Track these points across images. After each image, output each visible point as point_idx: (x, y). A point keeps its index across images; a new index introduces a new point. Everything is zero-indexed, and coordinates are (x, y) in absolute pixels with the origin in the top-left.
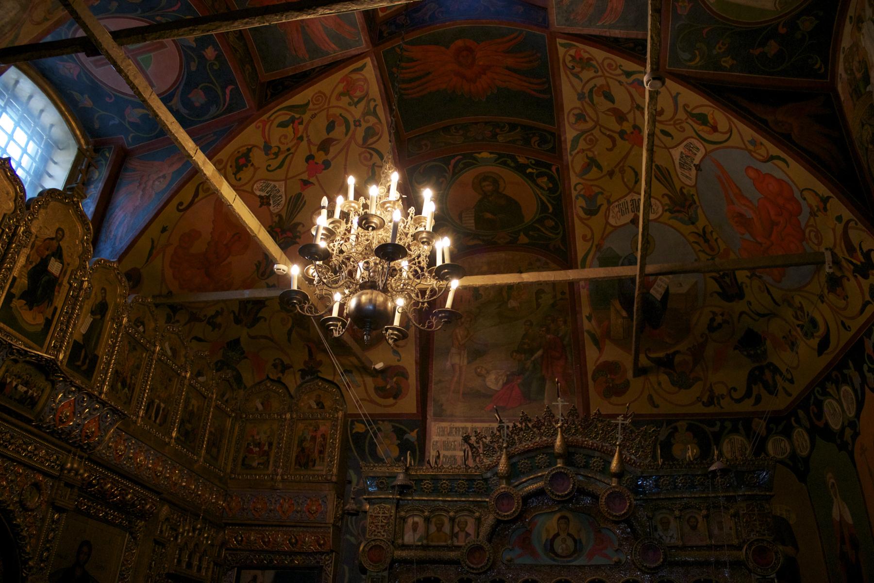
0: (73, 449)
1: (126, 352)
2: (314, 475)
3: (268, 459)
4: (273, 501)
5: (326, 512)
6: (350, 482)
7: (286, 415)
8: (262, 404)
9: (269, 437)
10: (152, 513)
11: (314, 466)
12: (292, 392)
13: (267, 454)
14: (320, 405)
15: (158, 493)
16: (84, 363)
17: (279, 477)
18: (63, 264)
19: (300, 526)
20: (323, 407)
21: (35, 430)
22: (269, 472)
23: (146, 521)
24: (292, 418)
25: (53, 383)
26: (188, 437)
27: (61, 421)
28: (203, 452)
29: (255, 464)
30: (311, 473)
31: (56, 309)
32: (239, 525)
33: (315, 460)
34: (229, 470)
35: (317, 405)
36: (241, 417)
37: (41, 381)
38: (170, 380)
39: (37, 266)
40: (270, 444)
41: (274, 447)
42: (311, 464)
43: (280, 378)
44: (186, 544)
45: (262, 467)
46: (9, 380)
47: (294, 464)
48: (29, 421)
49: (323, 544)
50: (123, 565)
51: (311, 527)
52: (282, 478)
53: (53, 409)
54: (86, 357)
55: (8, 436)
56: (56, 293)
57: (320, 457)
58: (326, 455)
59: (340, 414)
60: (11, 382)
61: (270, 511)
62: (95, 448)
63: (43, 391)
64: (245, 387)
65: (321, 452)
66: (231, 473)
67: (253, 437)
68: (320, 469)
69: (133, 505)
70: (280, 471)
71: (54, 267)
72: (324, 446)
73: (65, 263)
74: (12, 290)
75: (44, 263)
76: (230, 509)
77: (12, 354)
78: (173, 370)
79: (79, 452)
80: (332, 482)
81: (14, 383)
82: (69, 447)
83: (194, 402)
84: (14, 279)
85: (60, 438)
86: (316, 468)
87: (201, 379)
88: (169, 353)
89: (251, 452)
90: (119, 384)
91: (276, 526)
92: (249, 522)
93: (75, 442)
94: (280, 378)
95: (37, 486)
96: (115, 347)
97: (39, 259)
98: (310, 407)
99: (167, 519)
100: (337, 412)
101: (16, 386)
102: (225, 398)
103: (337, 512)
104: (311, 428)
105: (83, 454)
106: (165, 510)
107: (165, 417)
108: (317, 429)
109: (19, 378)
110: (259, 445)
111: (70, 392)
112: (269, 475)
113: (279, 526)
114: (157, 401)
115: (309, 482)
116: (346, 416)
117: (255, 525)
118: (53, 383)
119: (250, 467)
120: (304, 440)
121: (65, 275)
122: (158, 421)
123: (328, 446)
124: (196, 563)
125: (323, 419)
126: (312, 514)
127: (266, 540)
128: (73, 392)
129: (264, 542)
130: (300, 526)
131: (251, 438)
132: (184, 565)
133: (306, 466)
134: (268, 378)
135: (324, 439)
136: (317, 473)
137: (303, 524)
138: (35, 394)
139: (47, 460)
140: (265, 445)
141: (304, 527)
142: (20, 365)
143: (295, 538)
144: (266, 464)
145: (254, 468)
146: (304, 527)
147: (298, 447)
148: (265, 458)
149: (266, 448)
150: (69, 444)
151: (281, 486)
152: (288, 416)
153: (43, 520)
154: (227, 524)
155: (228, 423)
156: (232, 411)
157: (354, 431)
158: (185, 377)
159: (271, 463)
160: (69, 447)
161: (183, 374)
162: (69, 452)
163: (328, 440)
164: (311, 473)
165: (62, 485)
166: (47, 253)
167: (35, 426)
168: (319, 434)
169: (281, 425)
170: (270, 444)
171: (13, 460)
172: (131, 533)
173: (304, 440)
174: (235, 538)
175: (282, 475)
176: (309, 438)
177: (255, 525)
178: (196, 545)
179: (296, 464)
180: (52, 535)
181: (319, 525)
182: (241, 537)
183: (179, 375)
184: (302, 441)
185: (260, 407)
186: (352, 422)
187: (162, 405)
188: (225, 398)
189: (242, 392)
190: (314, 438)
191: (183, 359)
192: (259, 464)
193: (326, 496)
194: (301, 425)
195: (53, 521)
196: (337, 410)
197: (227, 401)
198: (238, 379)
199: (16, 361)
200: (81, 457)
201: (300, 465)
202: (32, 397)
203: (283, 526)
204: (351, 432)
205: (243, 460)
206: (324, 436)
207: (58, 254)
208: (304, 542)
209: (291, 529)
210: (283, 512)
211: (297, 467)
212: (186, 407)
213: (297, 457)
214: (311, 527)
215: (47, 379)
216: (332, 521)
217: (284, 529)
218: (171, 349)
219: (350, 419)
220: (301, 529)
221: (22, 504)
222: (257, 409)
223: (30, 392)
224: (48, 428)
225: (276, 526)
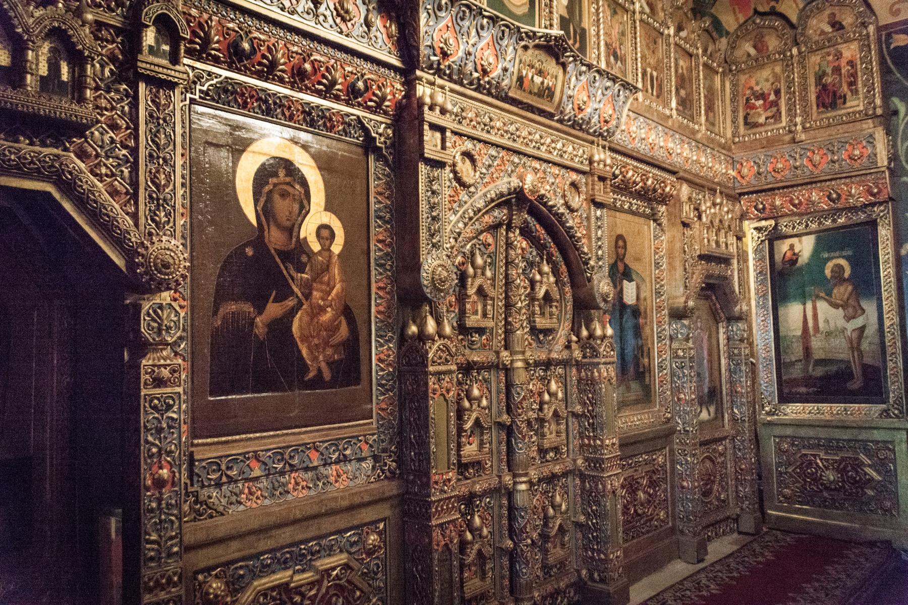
0: (596, 139)
1: (609, 18)
2: (849, 114)
3: (778, 110)
4: (798, 157)
5: (875, 155)
6: (896, 113)
7: (790, 50)
8: (755, 47)
9: (773, 84)
10: (672, 196)
11: (845, 103)
12: (794, 19)
13: (775, 104)
14: (837, 26)
15: (673, 173)
16: (575, 42)
17: (799, 127)
19: (841, 178)
20: (842, 27)
21: (558, 125)
22: (784, 124)
23: (666, 205)
24: (800, 53)
25: (564, 66)
26: (685, 104)
27: (579, 108)
28: (703, 118)
29: (762, 120)
30: (843, 111)
32: (756, 192)
33: (845, 96)
34: (729, 135)
35: (833, 26)
36: (731, 71)
37: (551, 66)
38: (655, 43)
40: (777, 92)
41: (783, 94)
42: (840, 101)
43: (773, 8)
44: (711, 222)
45: (772, 121)
46: (524, 72)
47: (815, 107)
48: (550, 116)
49: (878, 193)
50: (656, 253)
51: (856, 176)
52: (804, 128)
53: (570, 97)
54: (575, 32)
55: (537, 136)
57: (851, 91)
58: (860, 85)
59: (871, 29)
60: (527, 74)
61: (796, 168)
62: (614, 133)
63: (556, 77)
64: (728, 33)
65: (851, 84)
66: (734, 136)
67: (752, 88)
68: (856, 104)
69: (655, 190)
70: (798, 120)
72: (854, 75)
76: (743, 177)
77: (521, 39)
78: (655, 29)
79: (601, 142)
80: (877, 116)
81: (530, 75)
82: (590, 138)
83: (681, 63)
85: (581, 129)
86: (848, 104)
87: (683, 34)
88: (647, 10)
89: (753, 107)
90: (612, 58)
91: (807, 184)
92: (770, 186)
93: (595, 131)
94: (773, 8)
95: (574, 185)
96: (598, 14)
98: (823, 32)
99: (690, 199)
100: (866, 27)
101: (532, 77)
102: (709, 52)
103: (889, 152)
104: (831, 58)
105: (605, 143)
106: (685, 190)
107: (660, 87)
108: (839, 56)
109: (533, 67)
110: (763, 96)
112: (785, 128)
113: (811, 183)
114: (649, 70)
115: (844, 123)
116: (879, 29)
117: (778, 188)
118: (564, 66)
119: (756, 125)
120: (824, 74)
122: (655, 93)
123: (859, 74)
124: (722, 240)
125: (845, 42)
126: (856, 160)
127: (797, 202)
128: (585, 72)
129: (794, 205)
130: (841, 178)
131: (748, 92)
132: (714, 245)
133: (833, 106)
134: (756, 12)
135: (852, 67)
136: (851, 110)
137: (844, 175)
138: (551, 84)
139: (576, 156)
140: (770, 94)
141: (846, 178)
142: (530, 52)
143: (836, 192)
144: (777, 117)
145: (761, 125)
146: (846, 178)
147: (816, 86)
148: (774, 109)
149: (772, 97)
150: (589, 133)
151: (803, 137)
152: (795, 51)
153: (588, 218)
154: (741, 194)
155: (718, 79)
156: (719, 66)
157: (892, 47)
158: (669, 35)
159: (783, 113)
160: (590, 138)
161: (666, 32)
162: (592, 143)
163: (859, 66)
164: (843, 111)
165: (596, 179)
167: (558, 121)
168: (843, 62)
169: (787, 65)
170: (777, 92)
171: (548, 162)
172: (655, 221)
173: (824, 74)
174: (756, 207)
175: (803, 124)
176: (829, 70)
177: (778, 188)
178: (721, 221)
179: (818, 106)
180: (600, 233)
181: (868, 171)
182: (762, 203)
183: (662, 34)
184: (820, 77)
185: (753, 52)
186: (889, 36)
187: (655, 74)
188: (709, 52)
189: (724, 41)
190: (837, 70)
191: (662, 14)
192: (767, 118)
193: (871, 136)
194: (815, 59)
195: (597, 218)
196: (864, 25)
197: (711, 55)
198: (717, 24)
199: (526, 48)
200: (604, 147)
201: (824, 106)
202: (548, 88)
203: (816, 182)
204: (888, 48)
205: (745, 118)
206: (851, 63)
208: (851, 195)
209: (828, 183)
210: (814, 166)
211: (822, 109)
212: (676, 71)
213: (818, 97)
214: (856, 176)
215: (558, 63)
216: (886, 163)
217: (819, 185)
218: (648, 4)
219: (884, 33)
220: (843, 181)
221: (568, 207)
222: (749, 55)
223: (546, 81)
224: (569, 120)
225: (807, 184)
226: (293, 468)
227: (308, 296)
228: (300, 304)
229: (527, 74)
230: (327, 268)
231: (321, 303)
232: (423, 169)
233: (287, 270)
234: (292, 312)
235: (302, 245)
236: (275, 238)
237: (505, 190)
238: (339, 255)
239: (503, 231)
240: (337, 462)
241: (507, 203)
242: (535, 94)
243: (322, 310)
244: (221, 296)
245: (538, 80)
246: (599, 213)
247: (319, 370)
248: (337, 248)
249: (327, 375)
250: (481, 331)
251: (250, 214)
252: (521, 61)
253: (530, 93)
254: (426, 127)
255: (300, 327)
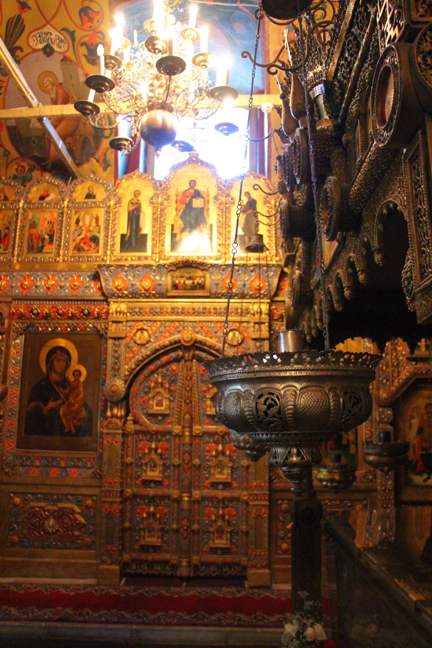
18: (203, 197)
31: (211, 226)
39: (184, 210)
56: (206, 217)
71: (197, 203)
73: (205, 196)
74: (175, 232)
75: (189, 205)
81: (182, 282)
84: (173, 226)
97: (184, 206)
101: (184, 283)
111: (224, 270)
121: (208, 202)
166: (188, 199)
202: (198, 284)
207: (197, 194)
215: (203, 270)
226: (53, 466)
227: (67, 399)
228: (64, 403)
229: (179, 282)
230: (77, 387)
231: (73, 402)
232: (110, 342)
233: (59, 389)
234: (59, 406)
235: (66, 380)
236: (54, 377)
237: (167, 343)
238: (84, 382)
239: (182, 363)
240: (75, 467)
241: (178, 348)
242: (189, 290)
243: (73, 405)
244: (30, 401)
245: (189, 282)
246: (258, 344)
247: (70, 429)
248: (82, 379)
249: (73, 431)
250: (164, 416)
251: (44, 370)
252: (173, 277)
253: (185, 289)
254: (110, 323)
255: (63, 411)
